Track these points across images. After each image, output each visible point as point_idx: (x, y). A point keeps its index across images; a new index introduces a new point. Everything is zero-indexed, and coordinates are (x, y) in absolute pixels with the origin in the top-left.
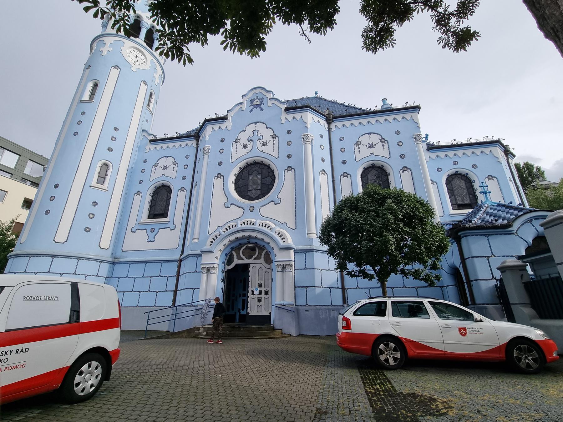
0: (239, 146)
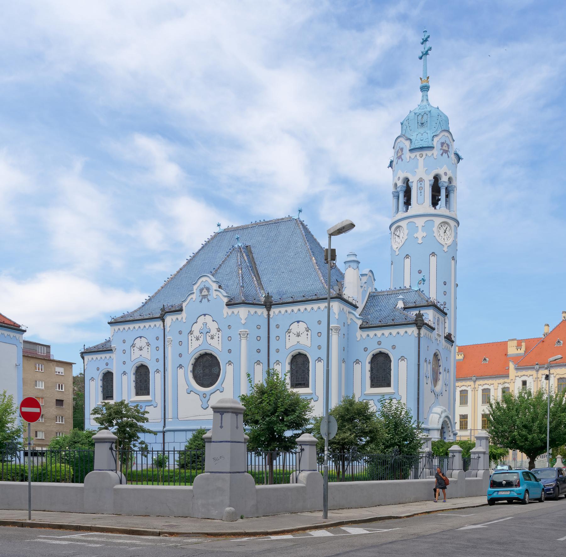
0: (193, 338)
